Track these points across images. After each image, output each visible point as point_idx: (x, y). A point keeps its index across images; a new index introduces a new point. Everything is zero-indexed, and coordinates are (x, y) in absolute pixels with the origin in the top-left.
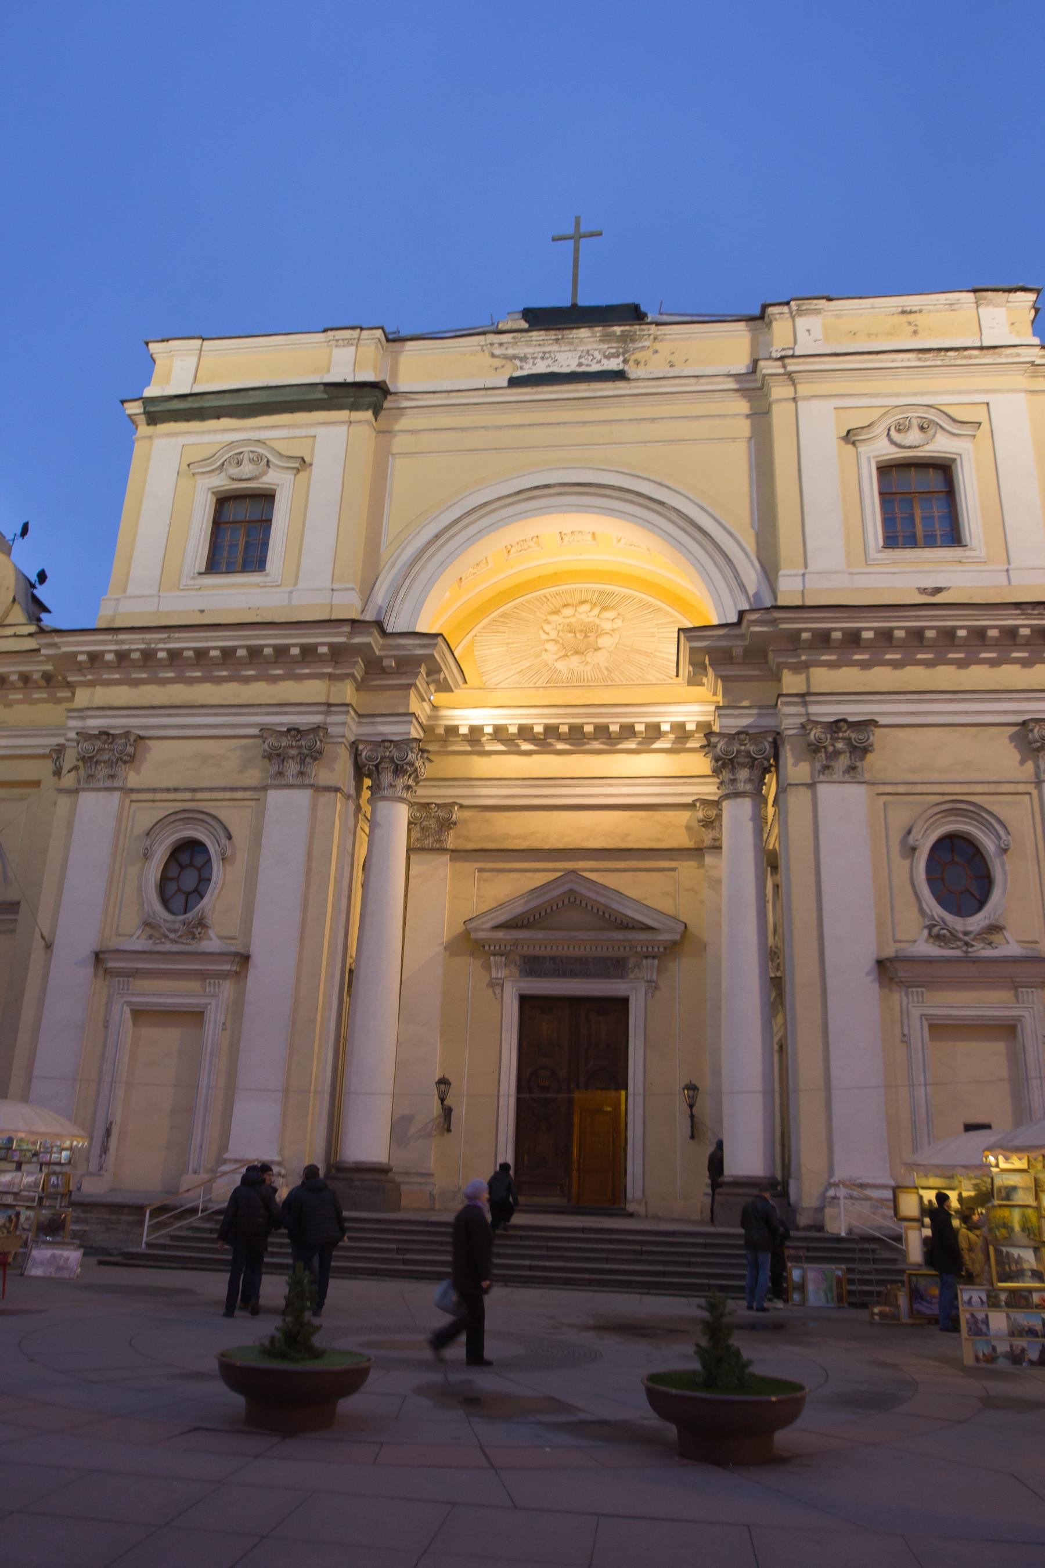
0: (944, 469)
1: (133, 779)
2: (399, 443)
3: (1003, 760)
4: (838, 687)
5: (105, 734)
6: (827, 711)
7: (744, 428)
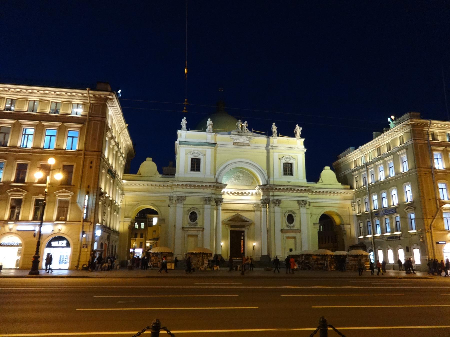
0: (291, 164)
1: (185, 203)
2: (218, 151)
3: (296, 205)
4: (278, 195)
6: (276, 198)
7: (266, 154)
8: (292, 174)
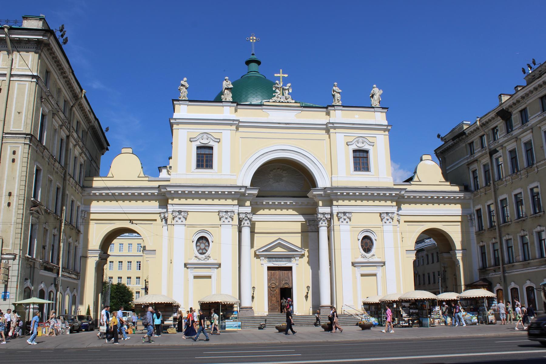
5: (180, 212)
8: (366, 168)
